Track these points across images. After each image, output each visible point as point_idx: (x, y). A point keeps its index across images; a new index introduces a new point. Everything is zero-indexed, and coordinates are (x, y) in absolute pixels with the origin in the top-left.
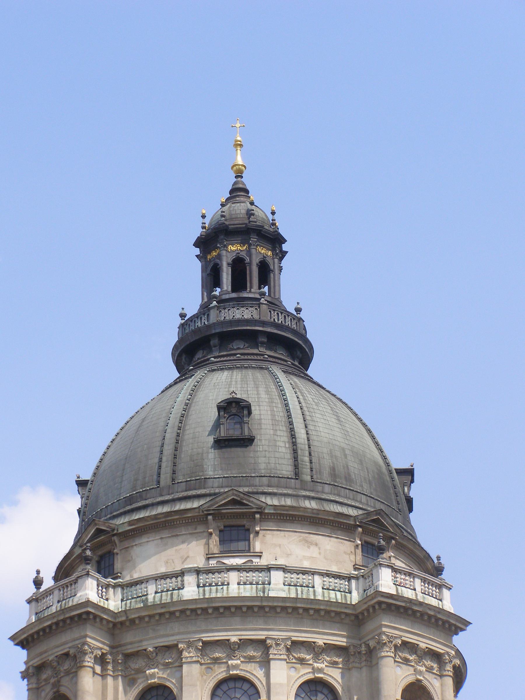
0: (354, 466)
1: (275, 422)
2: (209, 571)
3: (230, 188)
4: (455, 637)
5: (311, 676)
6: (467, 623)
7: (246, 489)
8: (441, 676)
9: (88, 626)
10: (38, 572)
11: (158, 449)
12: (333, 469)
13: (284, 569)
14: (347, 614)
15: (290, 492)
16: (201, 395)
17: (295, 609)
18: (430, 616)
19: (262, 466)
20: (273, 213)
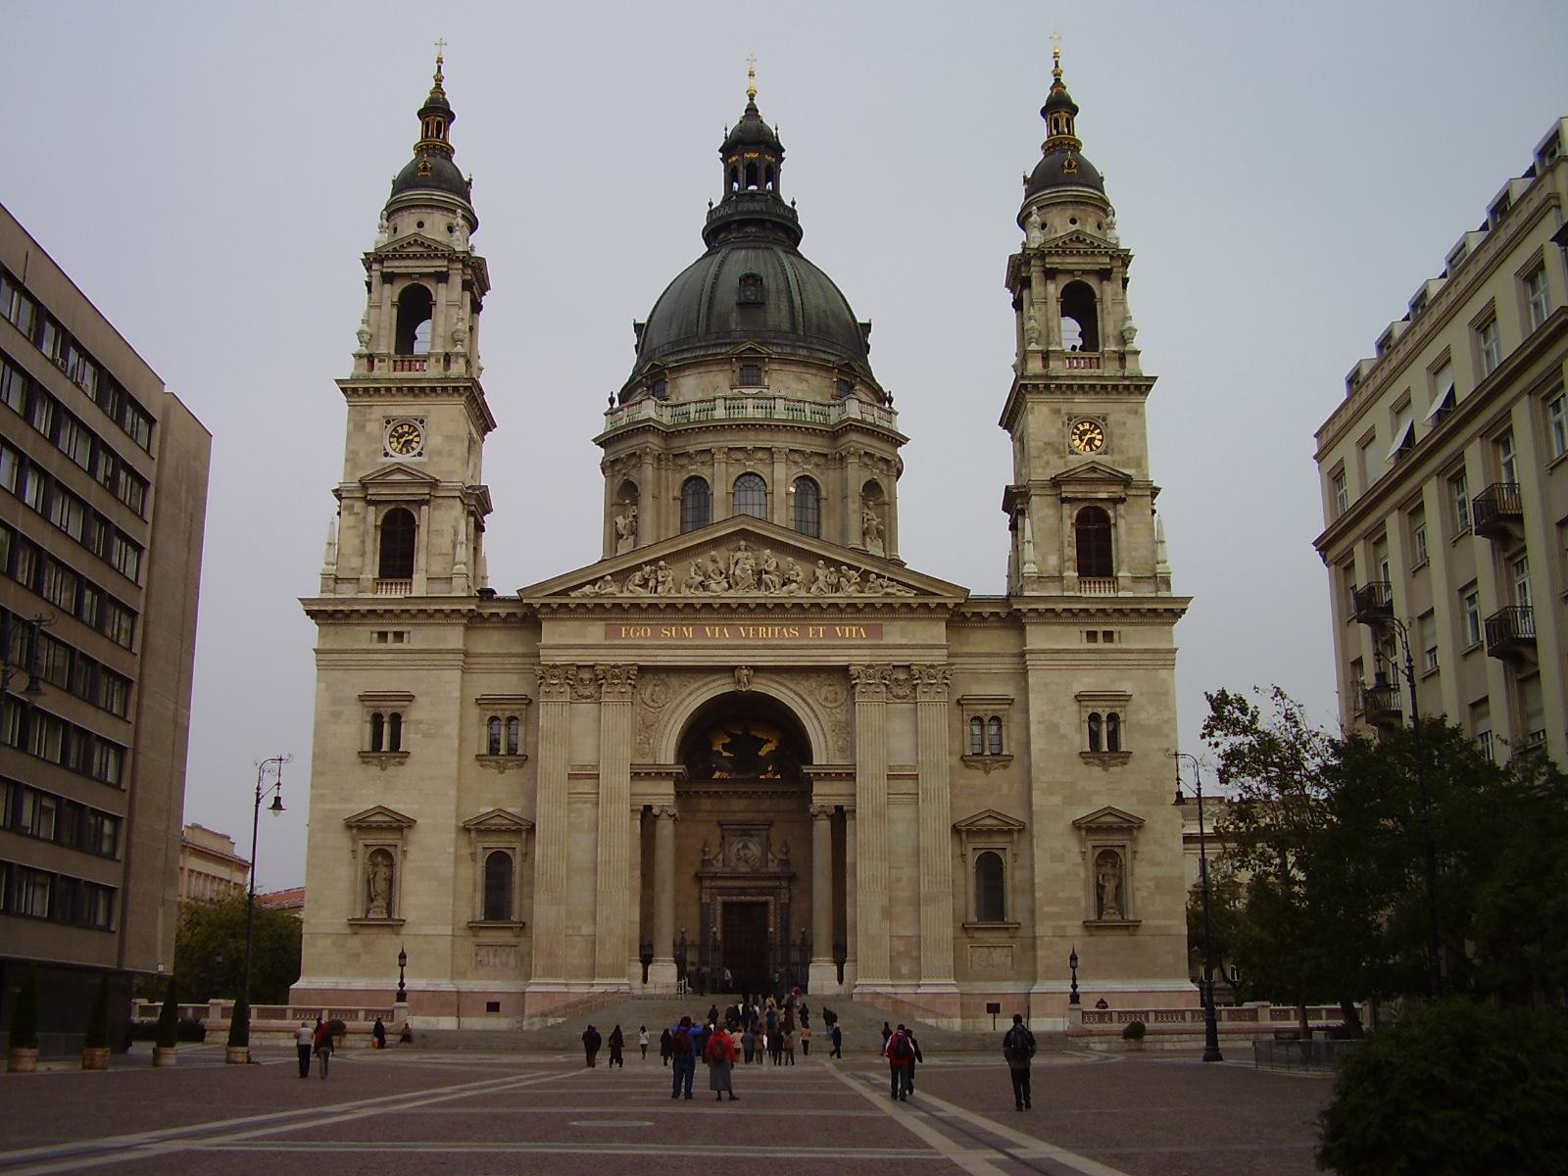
0: (832, 323)
1: (779, 291)
2: (734, 399)
3: (745, 107)
4: (899, 449)
5: (801, 474)
6: (908, 440)
7: (759, 340)
8: (889, 476)
9: (649, 435)
10: (612, 393)
11: (697, 308)
12: (818, 326)
13: (785, 399)
14: (827, 432)
15: (789, 343)
16: (726, 268)
17: (792, 427)
18: (884, 434)
19: (770, 323)
20: (776, 129)
